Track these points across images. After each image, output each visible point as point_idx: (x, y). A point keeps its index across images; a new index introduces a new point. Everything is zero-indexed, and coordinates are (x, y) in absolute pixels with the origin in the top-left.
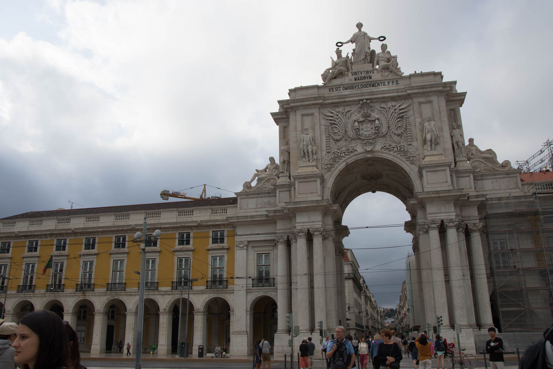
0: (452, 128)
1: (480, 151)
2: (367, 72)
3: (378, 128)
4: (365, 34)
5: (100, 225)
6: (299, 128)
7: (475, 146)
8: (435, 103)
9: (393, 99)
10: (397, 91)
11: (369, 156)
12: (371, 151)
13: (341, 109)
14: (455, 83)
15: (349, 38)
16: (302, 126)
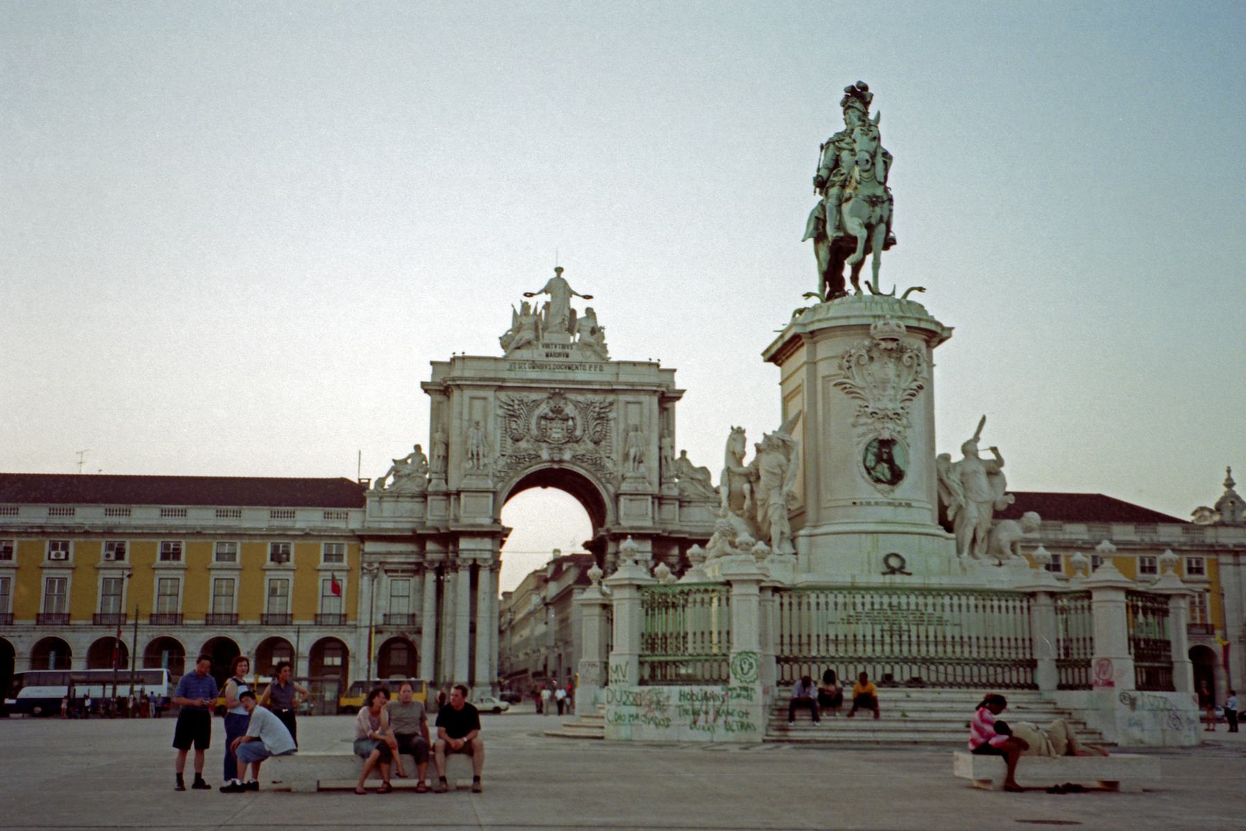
0: (661, 437)
1: (692, 468)
2: (564, 346)
3: (571, 431)
4: (565, 283)
5: (134, 523)
6: (466, 417)
7: (687, 461)
8: (646, 406)
9: (595, 391)
10: (601, 383)
11: (556, 466)
12: (561, 461)
13: (524, 395)
14: (675, 370)
15: (542, 287)
16: (470, 414)
